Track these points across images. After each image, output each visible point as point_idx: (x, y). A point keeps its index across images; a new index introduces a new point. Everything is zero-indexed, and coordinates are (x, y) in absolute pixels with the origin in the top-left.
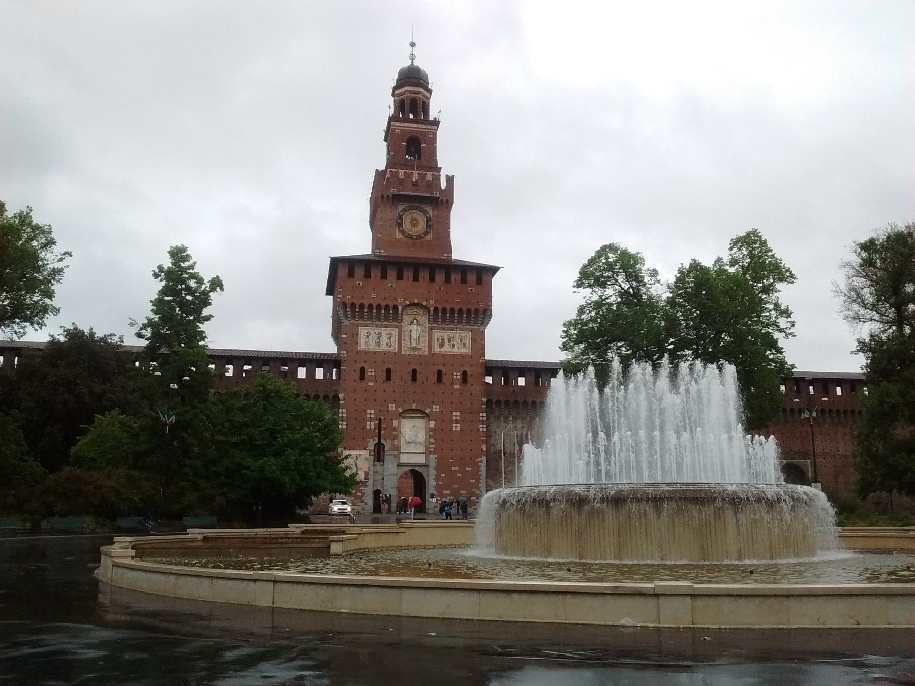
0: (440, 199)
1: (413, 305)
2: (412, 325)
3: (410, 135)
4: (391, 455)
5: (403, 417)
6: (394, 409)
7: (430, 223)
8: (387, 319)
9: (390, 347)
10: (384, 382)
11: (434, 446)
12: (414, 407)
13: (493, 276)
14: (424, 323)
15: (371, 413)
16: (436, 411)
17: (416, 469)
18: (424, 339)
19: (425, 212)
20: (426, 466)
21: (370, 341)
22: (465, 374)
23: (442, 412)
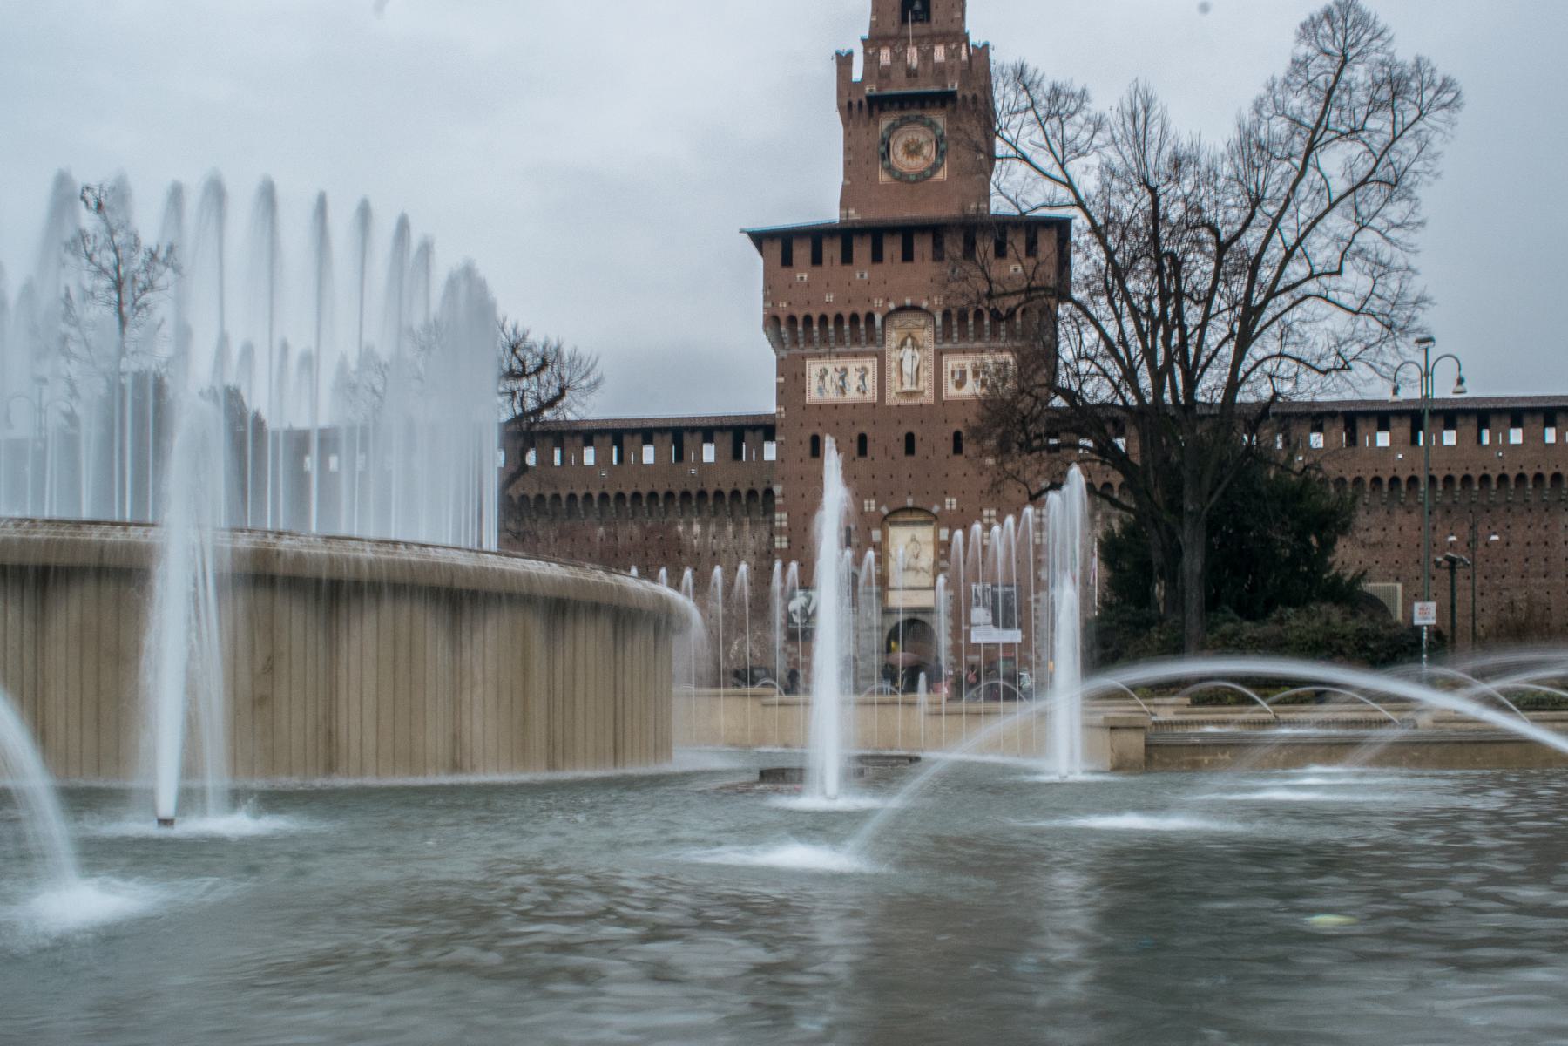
0: (959, 96)
1: (902, 309)
2: (904, 349)
6: (873, 508)
7: (943, 146)
8: (856, 340)
9: (864, 392)
10: (854, 459)
12: (910, 502)
14: (926, 344)
16: (951, 510)
18: (926, 374)
19: (932, 126)
23: (962, 510)
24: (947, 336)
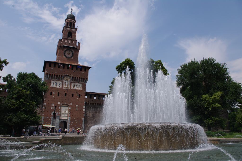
3: (70, 31)
4: (58, 116)
5: (62, 106)
11: (70, 114)
12: (65, 103)
13: (89, 69)
15: (53, 104)
17: (65, 120)
19: (72, 51)
20: (67, 120)
21: (54, 85)
22: (80, 95)
24: (72, 80)
